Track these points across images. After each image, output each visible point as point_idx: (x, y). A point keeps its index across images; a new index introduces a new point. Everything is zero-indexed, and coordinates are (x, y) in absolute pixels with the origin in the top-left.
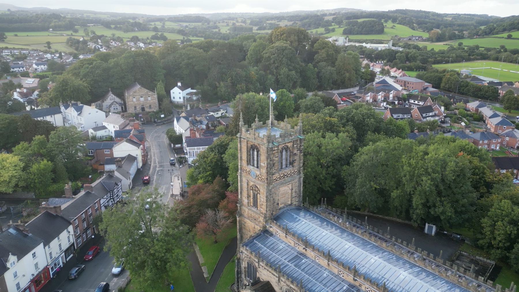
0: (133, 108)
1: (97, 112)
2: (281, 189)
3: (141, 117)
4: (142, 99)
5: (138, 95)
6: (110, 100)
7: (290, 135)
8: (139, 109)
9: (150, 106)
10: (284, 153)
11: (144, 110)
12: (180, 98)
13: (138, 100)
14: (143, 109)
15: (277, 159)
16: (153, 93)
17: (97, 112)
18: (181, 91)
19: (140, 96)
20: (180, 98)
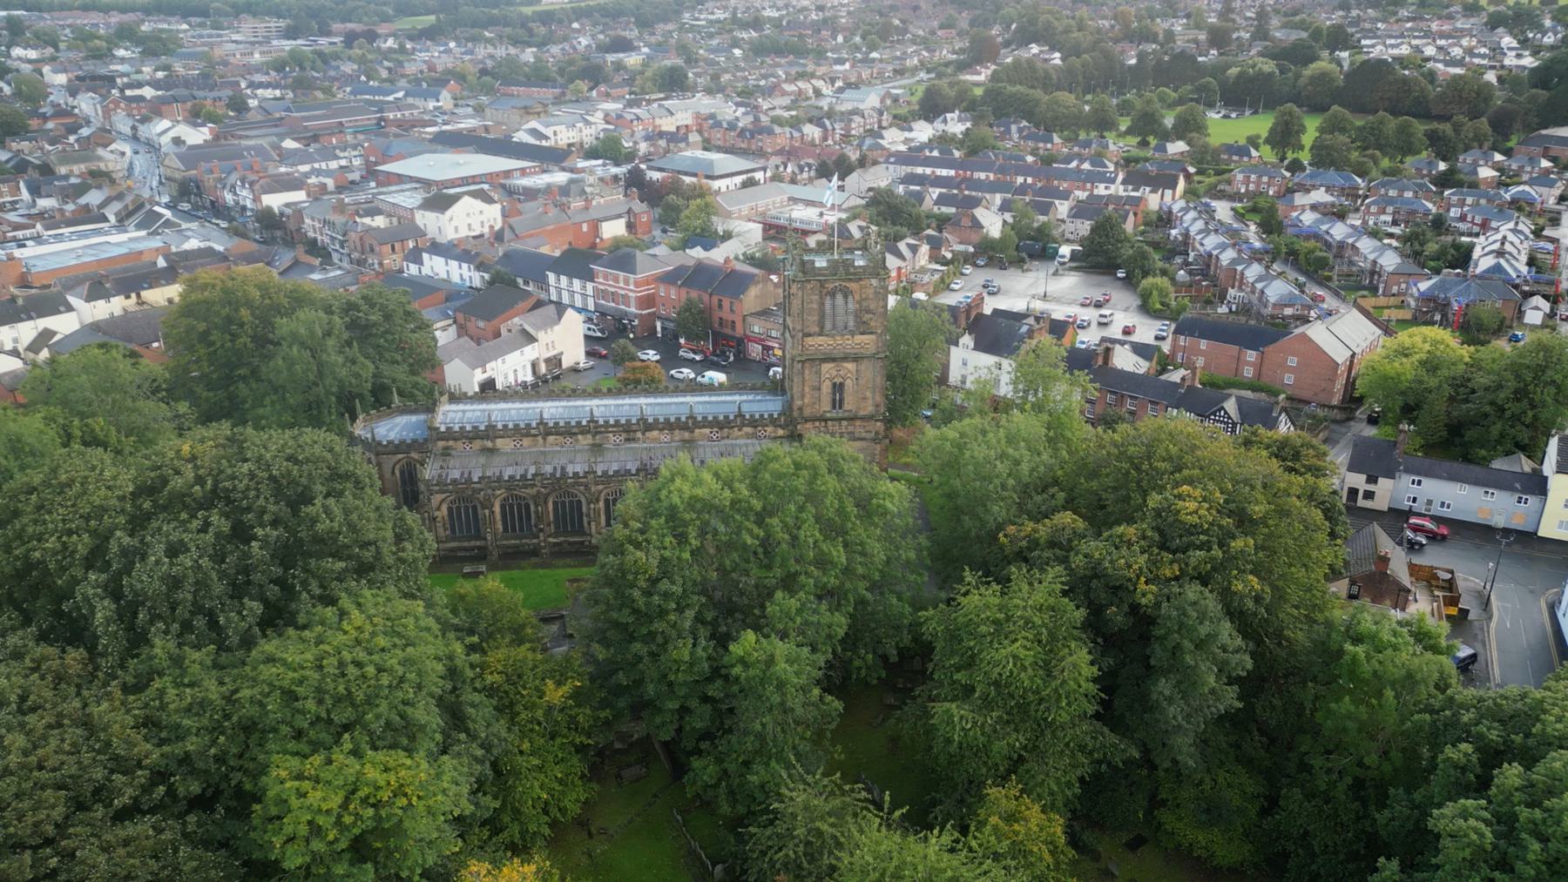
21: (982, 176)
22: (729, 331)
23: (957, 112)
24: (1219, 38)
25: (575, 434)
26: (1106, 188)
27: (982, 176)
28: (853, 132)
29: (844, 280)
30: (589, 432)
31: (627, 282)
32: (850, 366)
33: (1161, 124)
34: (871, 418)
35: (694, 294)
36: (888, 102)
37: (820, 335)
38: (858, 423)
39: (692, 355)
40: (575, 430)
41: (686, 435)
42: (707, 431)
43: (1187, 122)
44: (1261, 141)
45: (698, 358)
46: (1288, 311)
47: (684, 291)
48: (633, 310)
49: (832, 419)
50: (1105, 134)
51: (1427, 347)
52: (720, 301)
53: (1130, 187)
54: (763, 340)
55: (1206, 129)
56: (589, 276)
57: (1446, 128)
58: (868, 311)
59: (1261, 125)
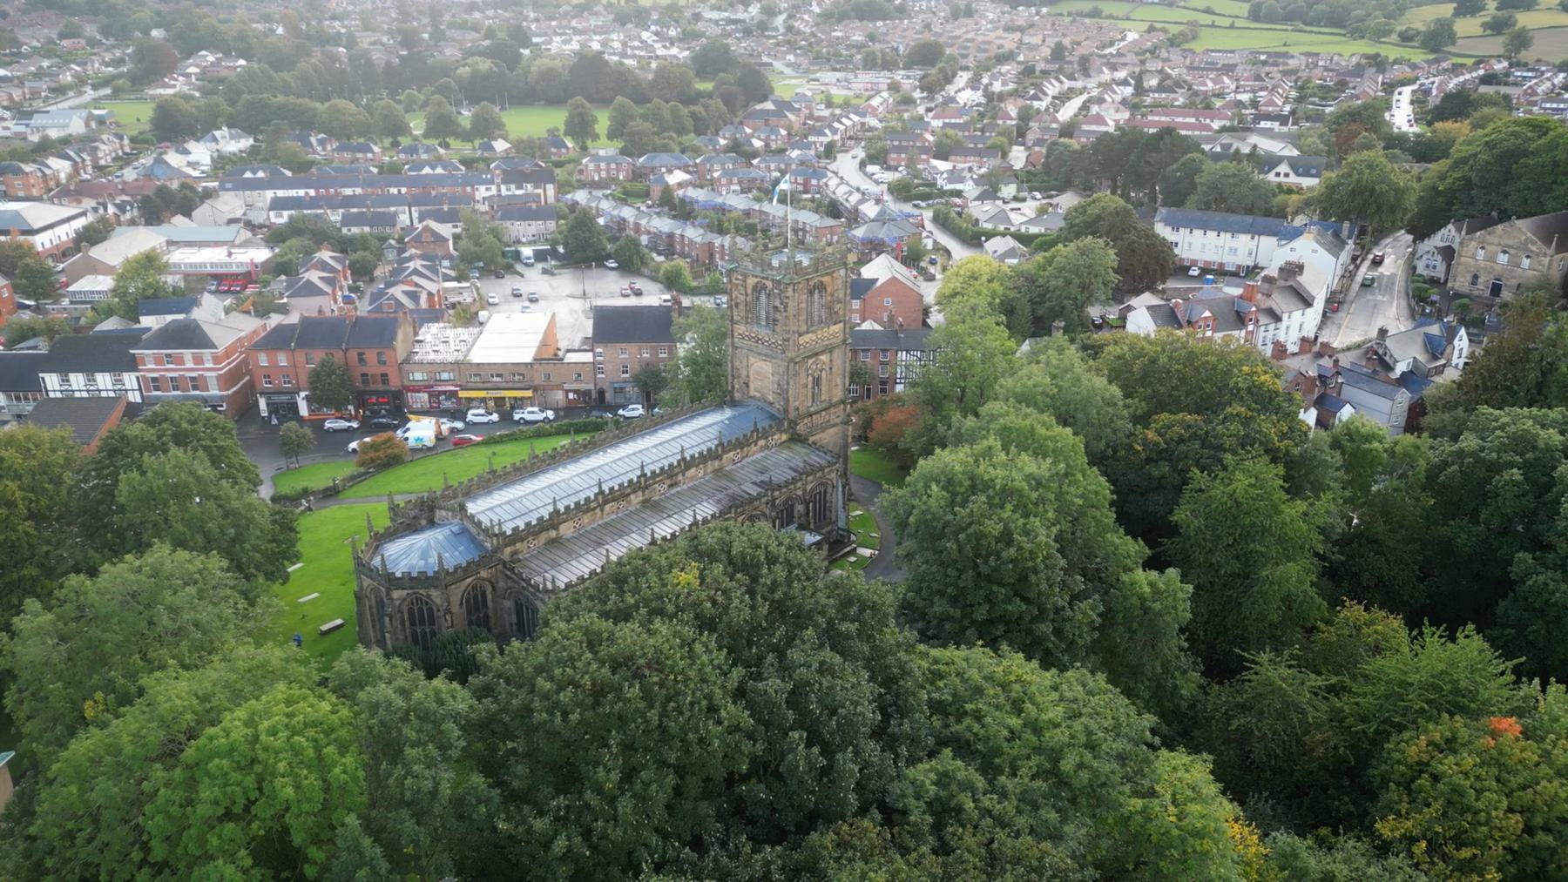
0: (1469, 277)
1: (1315, 251)
2: (752, 360)
3: (1433, 303)
4: (1503, 259)
5: (1496, 241)
6: (1442, 240)
8: (1483, 288)
10: (763, 298)
11: (1498, 296)
13: (1491, 258)
14: (1496, 290)
15: (742, 298)
17: (1315, 251)
21: (348, 192)
22: (380, 387)
23: (225, 128)
24: (408, 40)
25: (628, 495)
26: (487, 189)
27: (348, 192)
28: (102, 162)
29: (822, 275)
30: (640, 488)
31: (198, 360)
32: (823, 358)
33: (459, 125)
34: (843, 402)
35: (319, 355)
36: (94, 125)
37: (808, 332)
38: (832, 410)
39: (343, 424)
40: (628, 491)
41: (716, 464)
42: (731, 454)
43: (486, 120)
44: (561, 133)
45: (355, 425)
47: (300, 356)
51: (987, 269)
52: (360, 354)
53: (513, 186)
54: (432, 387)
55: (504, 126)
56: (132, 365)
57: (698, 108)
58: (839, 302)
59: (557, 119)
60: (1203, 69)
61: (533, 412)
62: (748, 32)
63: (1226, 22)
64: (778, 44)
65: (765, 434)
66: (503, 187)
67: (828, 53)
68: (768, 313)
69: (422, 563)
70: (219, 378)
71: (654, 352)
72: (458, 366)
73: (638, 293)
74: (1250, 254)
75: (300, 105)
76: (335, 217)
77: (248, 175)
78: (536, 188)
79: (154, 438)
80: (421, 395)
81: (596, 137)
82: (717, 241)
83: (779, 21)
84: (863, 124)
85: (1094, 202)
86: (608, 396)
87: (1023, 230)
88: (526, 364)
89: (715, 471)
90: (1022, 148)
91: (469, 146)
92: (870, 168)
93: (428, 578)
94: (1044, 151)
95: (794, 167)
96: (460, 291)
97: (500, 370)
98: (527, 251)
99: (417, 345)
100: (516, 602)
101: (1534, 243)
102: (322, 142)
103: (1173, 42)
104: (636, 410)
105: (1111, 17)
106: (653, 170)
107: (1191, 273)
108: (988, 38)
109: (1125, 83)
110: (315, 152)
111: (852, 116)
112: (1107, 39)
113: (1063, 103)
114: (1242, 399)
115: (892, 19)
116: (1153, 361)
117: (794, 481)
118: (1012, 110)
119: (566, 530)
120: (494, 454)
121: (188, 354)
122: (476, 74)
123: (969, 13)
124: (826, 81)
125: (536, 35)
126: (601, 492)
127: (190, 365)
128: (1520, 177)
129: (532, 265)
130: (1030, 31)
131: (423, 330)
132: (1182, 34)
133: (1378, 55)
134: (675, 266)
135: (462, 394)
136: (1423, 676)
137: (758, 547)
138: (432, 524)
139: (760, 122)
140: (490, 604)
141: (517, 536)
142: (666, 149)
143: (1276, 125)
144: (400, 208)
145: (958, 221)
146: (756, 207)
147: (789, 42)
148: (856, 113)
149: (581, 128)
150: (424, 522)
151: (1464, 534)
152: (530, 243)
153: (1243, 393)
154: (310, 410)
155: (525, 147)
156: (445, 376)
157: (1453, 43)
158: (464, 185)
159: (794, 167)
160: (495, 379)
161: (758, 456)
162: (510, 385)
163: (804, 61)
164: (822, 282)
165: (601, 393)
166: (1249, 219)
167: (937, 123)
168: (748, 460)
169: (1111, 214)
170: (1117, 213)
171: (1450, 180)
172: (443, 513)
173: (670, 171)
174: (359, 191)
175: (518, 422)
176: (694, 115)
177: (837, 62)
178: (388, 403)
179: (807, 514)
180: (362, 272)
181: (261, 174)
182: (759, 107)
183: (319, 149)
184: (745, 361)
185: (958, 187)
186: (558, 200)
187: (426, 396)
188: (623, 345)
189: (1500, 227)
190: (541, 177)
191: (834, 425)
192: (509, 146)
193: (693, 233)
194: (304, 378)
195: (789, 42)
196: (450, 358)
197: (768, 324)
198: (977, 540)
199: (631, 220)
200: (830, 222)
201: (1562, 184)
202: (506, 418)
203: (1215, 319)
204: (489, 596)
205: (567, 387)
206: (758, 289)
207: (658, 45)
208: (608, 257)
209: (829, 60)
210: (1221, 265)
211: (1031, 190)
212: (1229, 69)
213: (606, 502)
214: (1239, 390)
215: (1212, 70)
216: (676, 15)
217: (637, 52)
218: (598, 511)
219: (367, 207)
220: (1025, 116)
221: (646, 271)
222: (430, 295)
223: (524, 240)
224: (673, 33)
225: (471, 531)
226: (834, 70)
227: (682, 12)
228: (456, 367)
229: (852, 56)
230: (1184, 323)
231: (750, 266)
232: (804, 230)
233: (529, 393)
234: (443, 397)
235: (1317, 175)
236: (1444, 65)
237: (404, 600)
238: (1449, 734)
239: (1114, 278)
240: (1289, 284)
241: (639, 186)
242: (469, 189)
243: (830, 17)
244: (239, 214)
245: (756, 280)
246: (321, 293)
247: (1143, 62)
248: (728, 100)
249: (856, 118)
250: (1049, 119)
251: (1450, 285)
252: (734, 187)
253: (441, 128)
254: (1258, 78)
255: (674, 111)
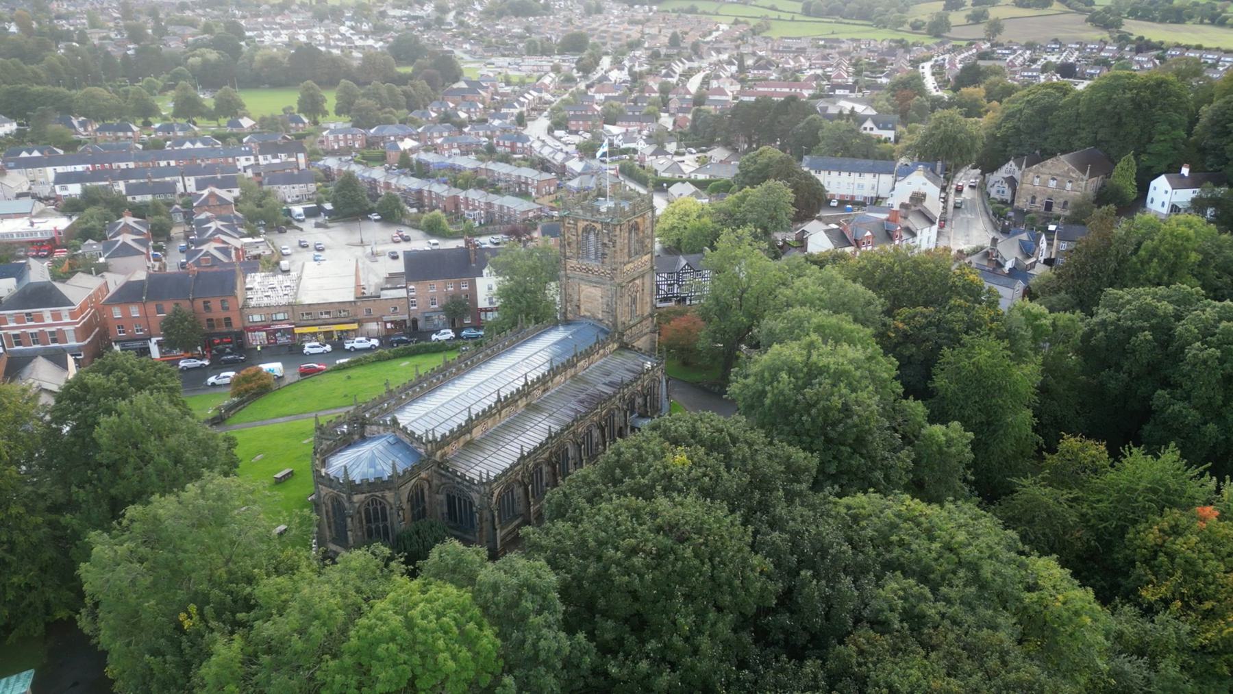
0: (1029, 198)
2: (583, 287)
3: (1009, 218)
4: (1053, 184)
7: (598, 210)
8: (1039, 205)
9: (1066, 203)
10: (592, 237)
12: (1163, 204)
13: (1045, 184)
14: (1049, 206)
15: (574, 238)
16: (1081, 176)
18: (1169, 188)
19: (1050, 177)
20: (1163, 204)
21: (123, 165)
22: (225, 329)
24: (136, 35)
25: (517, 401)
26: (247, 160)
27: (123, 165)
31: (56, 316)
32: (637, 282)
33: (204, 106)
38: (644, 323)
40: (517, 397)
41: (573, 370)
44: (296, 110)
45: (206, 363)
46: (531, 214)
47: (151, 307)
48: (73, 343)
49: (635, 325)
50: (151, 119)
53: (269, 157)
54: (269, 326)
55: (244, 106)
57: (408, 88)
58: (648, 237)
60: (782, 52)
61: (361, 342)
62: (428, 26)
63: (789, 17)
64: (454, 36)
65: (603, 345)
66: (261, 158)
67: (497, 42)
68: (596, 249)
69: (372, 470)
70: (76, 330)
71: (458, 286)
72: (292, 307)
73: (407, 239)
74: (873, 188)
75: (57, 93)
76: (121, 186)
77: (24, 154)
78: (289, 157)
79: (115, 385)
80: (260, 333)
81: (325, 113)
82: (462, 195)
83: (450, 17)
84: (540, 98)
85: (761, 153)
86: (420, 324)
87: (693, 177)
88: (350, 302)
89: (572, 377)
90: (667, 115)
91: (214, 123)
92: (558, 133)
93: (383, 482)
94: (690, 116)
95: (498, 133)
96: (256, 245)
97: (328, 307)
98: (298, 210)
99: (249, 292)
100: (448, 496)
101: (1074, 172)
102: (83, 124)
103: (754, 32)
104: (447, 334)
105: (704, 13)
106: (383, 138)
107: (832, 204)
108: (618, 30)
109: (730, 63)
110: (77, 133)
111: (531, 92)
112: (706, 29)
113: (688, 79)
114: (958, 294)
115: (541, 15)
116: (891, 269)
117: (636, 380)
118: (654, 84)
119: (477, 433)
120: (349, 378)
121: (47, 312)
122: (206, 63)
123: (599, 10)
124: (500, 64)
125: (249, 30)
126: (499, 400)
127: (49, 321)
128: (1054, 125)
129: (303, 221)
130: (649, 24)
131: (248, 280)
132: (759, 25)
133: (903, 40)
134: (433, 216)
135: (297, 331)
136: (1143, 484)
137: (721, 431)
138: (364, 439)
139: (458, 98)
140: (426, 499)
141: (445, 441)
142: (389, 122)
143: (847, 92)
144: (175, 178)
145: (642, 172)
146: (483, 166)
147: (463, 34)
148: (535, 90)
149: (312, 106)
150: (356, 437)
151: (1114, 382)
152: (298, 202)
153: (960, 289)
154: (161, 352)
155: (268, 125)
156: (280, 316)
157: (949, 30)
158: (226, 157)
159: (498, 133)
160: (324, 316)
161: (599, 362)
162: (337, 320)
163: (480, 50)
164: (636, 223)
165: (415, 322)
166: (870, 162)
167: (600, 97)
168: (593, 366)
169: (778, 162)
170: (783, 162)
171: (1003, 129)
172: (375, 428)
173: (402, 140)
174: (132, 165)
175: (349, 350)
176: (405, 93)
177: (505, 49)
178: (230, 343)
179: (645, 405)
180: (160, 234)
181: (36, 154)
182: (455, 86)
183: (81, 130)
184: (576, 288)
185: (632, 145)
186: (308, 166)
187: (264, 333)
188: (431, 282)
189: (1049, 161)
190: (295, 145)
191: (646, 334)
192: (253, 123)
193: (440, 189)
194: (155, 326)
195: (463, 34)
196: (284, 301)
197: (596, 258)
198: (826, 414)
199: (382, 180)
200: (546, 176)
201: (1084, 129)
202: (339, 348)
203: (874, 237)
204: (426, 492)
205: (385, 319)
206: (587, 230)
207: (355, 38)
208: (371, 211)
209: (499, 48)
210: (853, 197)
211: (687, 146)
212: (801, 51)
213: (503, 408)
214: (956, 287)
215: (790, 52)
216: (366, 13)
217: (339, 43)
218: (497, 416)
219: (149, 178)
220: (665, 90)
221: (407, 221)
222: (236, 249)
223: (289, 200)
224: (365, 27)
225: (404, 440)
226: (504, 55)
227: (370, 10)
228: (290, 309)
229: (515, 45)
230: (852, 242)
231: (581, 212)
232: (526, 184)
233: (355, 326)
234: (279, 334)
235: (893, 129)
236: (948, 46)
237: (363, 502)
238: (1173, 523)
239: (793, 210)
240: (917, 208)
241: (376, 152)
242: (230, 160)
243: (491, 14)
244: (25, 189)
245: (586, 223)
246: (138, 253)
247: (738, 47)
248: (431, 81)
249: (535, 94)
250: (683, 91)
251: (1016, 204)
252: (454, 151)
253: (188, 109)
254: (825, 57)
255: (391, 92)
